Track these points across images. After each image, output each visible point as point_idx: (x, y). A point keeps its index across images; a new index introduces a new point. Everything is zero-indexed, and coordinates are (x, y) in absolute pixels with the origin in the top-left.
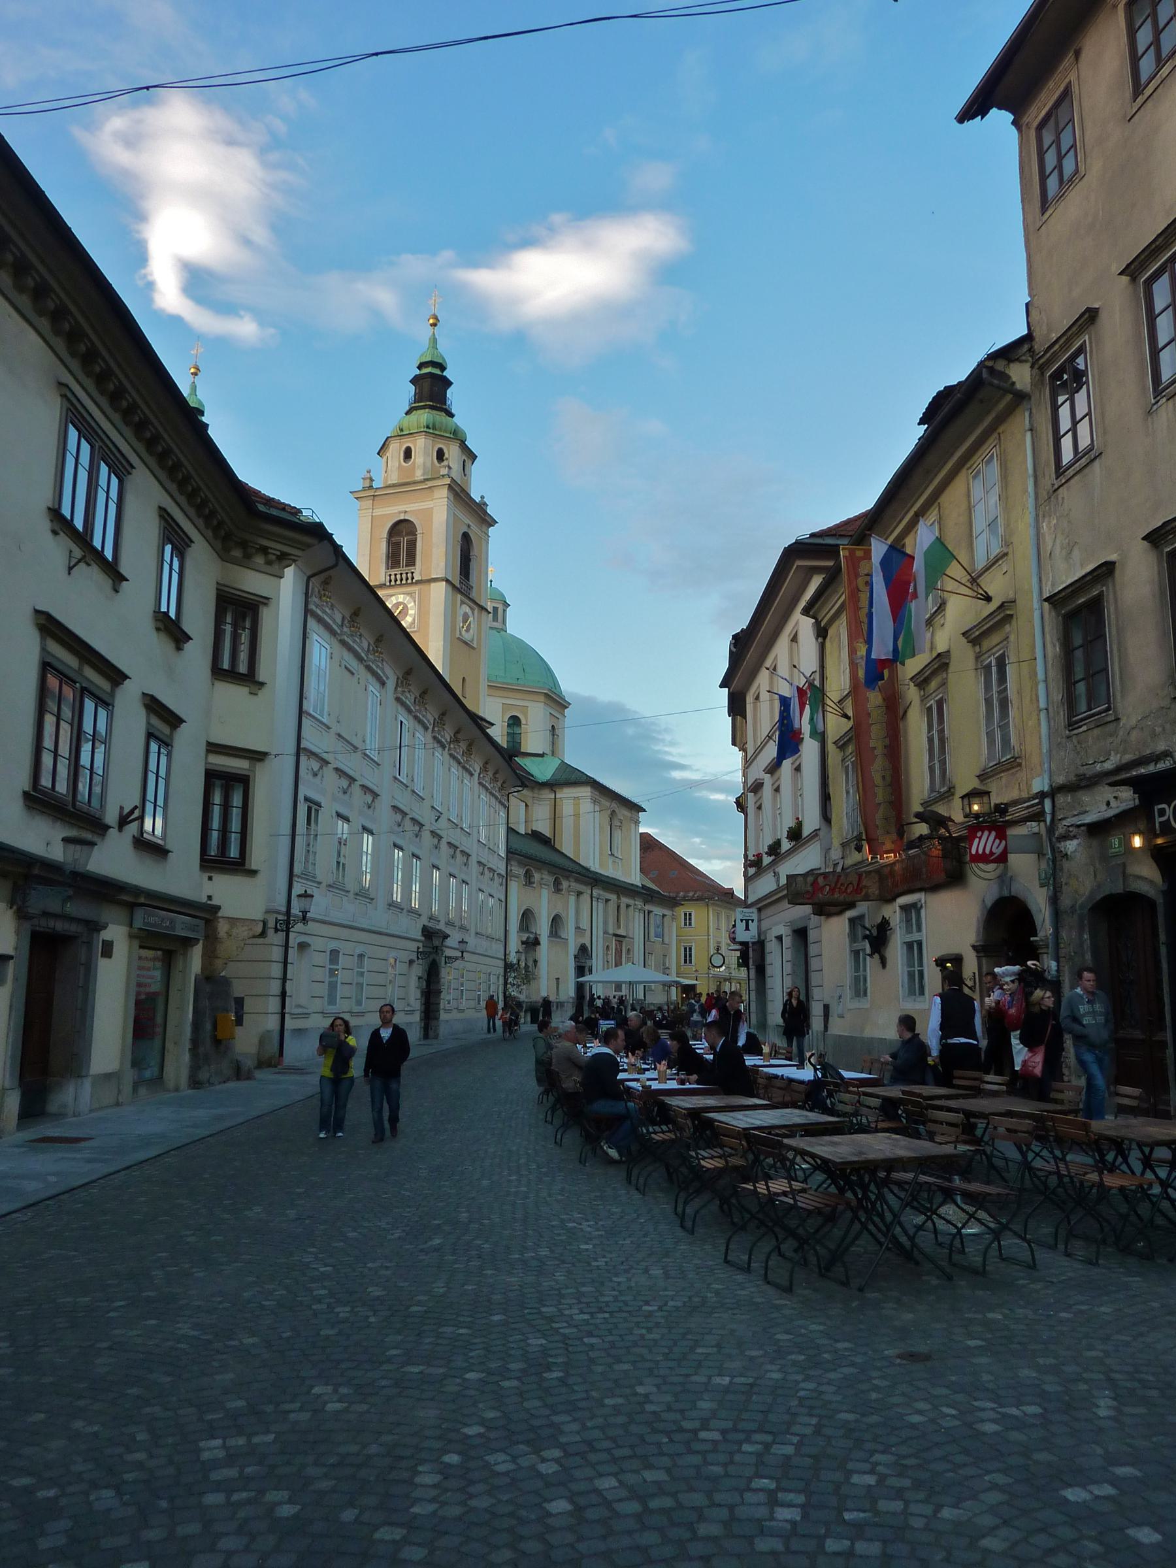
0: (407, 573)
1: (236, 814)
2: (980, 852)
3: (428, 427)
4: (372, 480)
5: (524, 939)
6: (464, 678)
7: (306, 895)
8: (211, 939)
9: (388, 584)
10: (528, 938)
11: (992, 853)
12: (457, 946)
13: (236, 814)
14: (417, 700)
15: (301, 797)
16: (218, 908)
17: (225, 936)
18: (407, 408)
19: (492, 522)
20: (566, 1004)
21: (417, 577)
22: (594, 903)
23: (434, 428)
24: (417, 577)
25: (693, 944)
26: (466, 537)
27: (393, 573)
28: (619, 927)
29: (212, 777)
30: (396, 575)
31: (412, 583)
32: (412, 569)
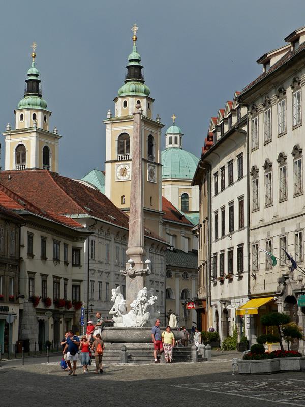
1: (78, 293)
3: (133, 91)
6: (151, 198)
7: (92, 305)
8: (74, 318)
13: (78, 293)
23: (136, 91)
26: (151, 138)
29: (73, 286)
31: (128, 160)
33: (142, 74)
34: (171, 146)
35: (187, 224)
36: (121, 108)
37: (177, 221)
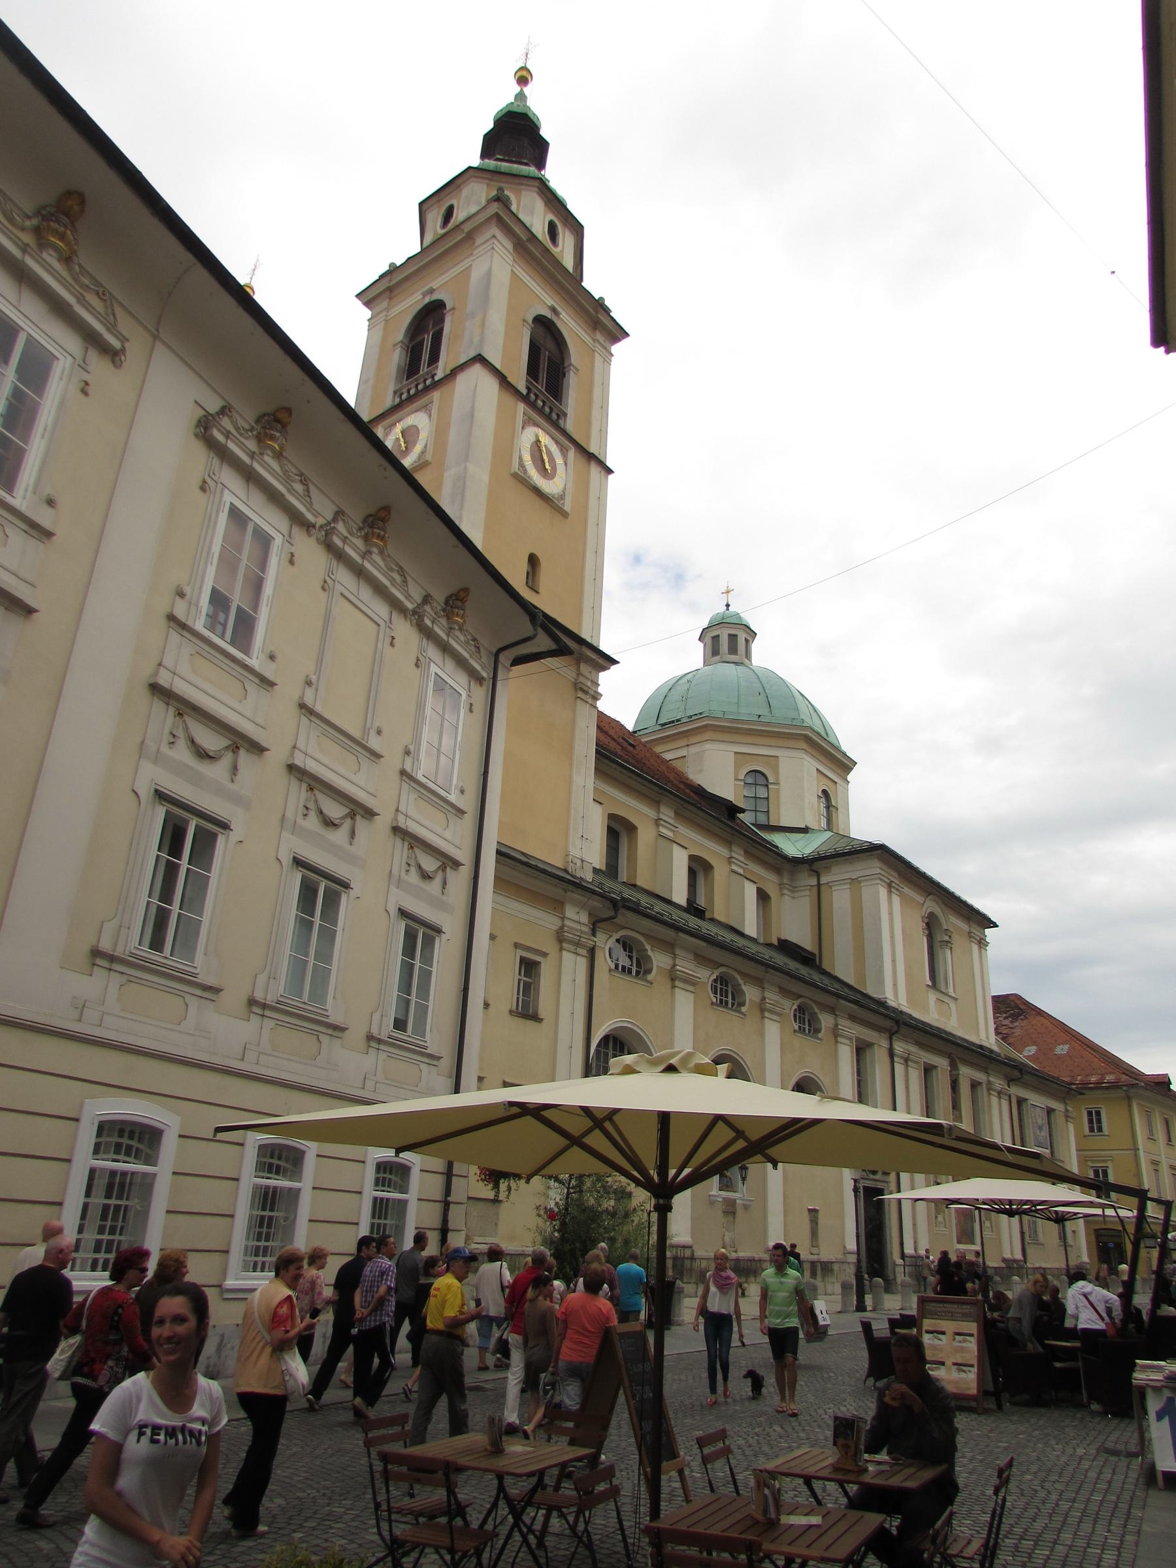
19: (617, 333)
20: (836, 1267)
22: (899, 1068)
25: (1109, 1164)
28: (959, 1118)
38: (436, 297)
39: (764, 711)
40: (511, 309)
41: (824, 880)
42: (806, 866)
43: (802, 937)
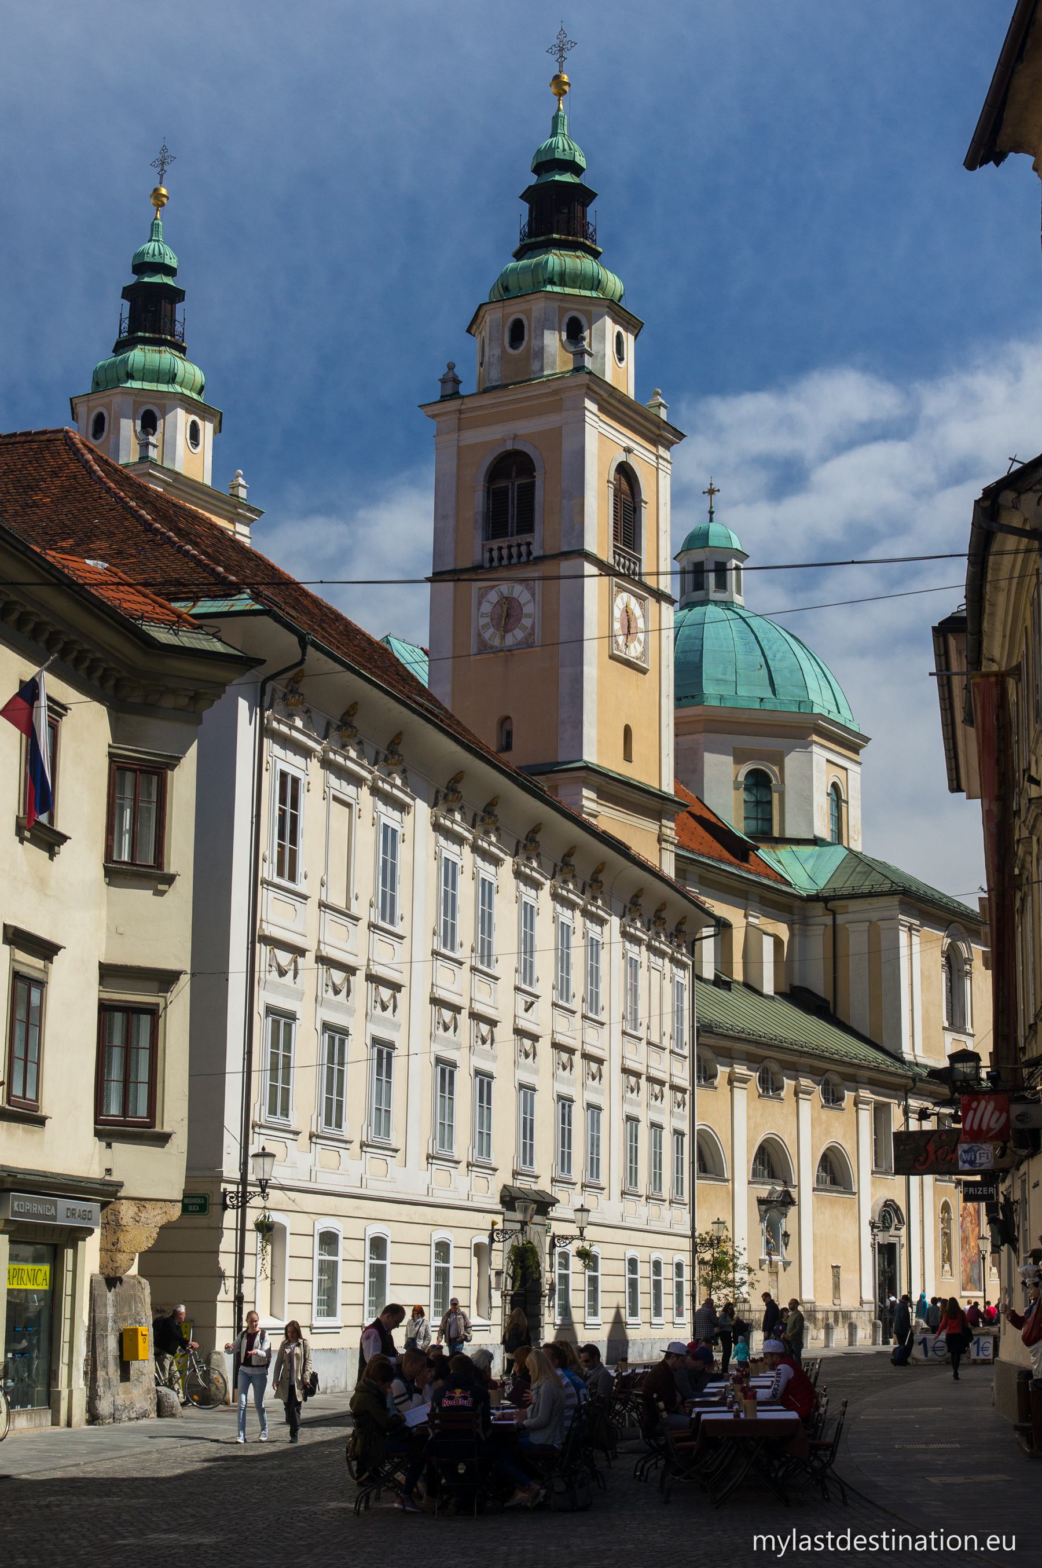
0: (519, 545)
2: (975, 1127)
4: (457, 382)
5: (764, 1195)
6: (627, 731)
7: (264, 1154)
8: (113, 1227)
9: (487, 565)
10: (771, 1193)
11: (989, 1129)
12: (571, 1215)
14: (478, 819)
15: (259, 1009)
16: (120, 1185)
17: (131, 1222)
18: (517, 245)
21: (537, 552)
24: (537, 552)
26: (625, 472)
27: (495, 547)
30: (500, 549)
31: (528, 562)
32: (526, 537)
33: (590, 219)
34: (699, 595)
35: (767, 877)
36: (497, 352)
37: (731, 864)
38: (519, 447)
39: (768, 693)
40: (600, 474)
41: (840, 919)
42: (822, 905)
43: (818, 983)
